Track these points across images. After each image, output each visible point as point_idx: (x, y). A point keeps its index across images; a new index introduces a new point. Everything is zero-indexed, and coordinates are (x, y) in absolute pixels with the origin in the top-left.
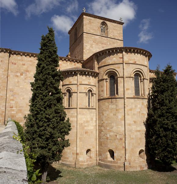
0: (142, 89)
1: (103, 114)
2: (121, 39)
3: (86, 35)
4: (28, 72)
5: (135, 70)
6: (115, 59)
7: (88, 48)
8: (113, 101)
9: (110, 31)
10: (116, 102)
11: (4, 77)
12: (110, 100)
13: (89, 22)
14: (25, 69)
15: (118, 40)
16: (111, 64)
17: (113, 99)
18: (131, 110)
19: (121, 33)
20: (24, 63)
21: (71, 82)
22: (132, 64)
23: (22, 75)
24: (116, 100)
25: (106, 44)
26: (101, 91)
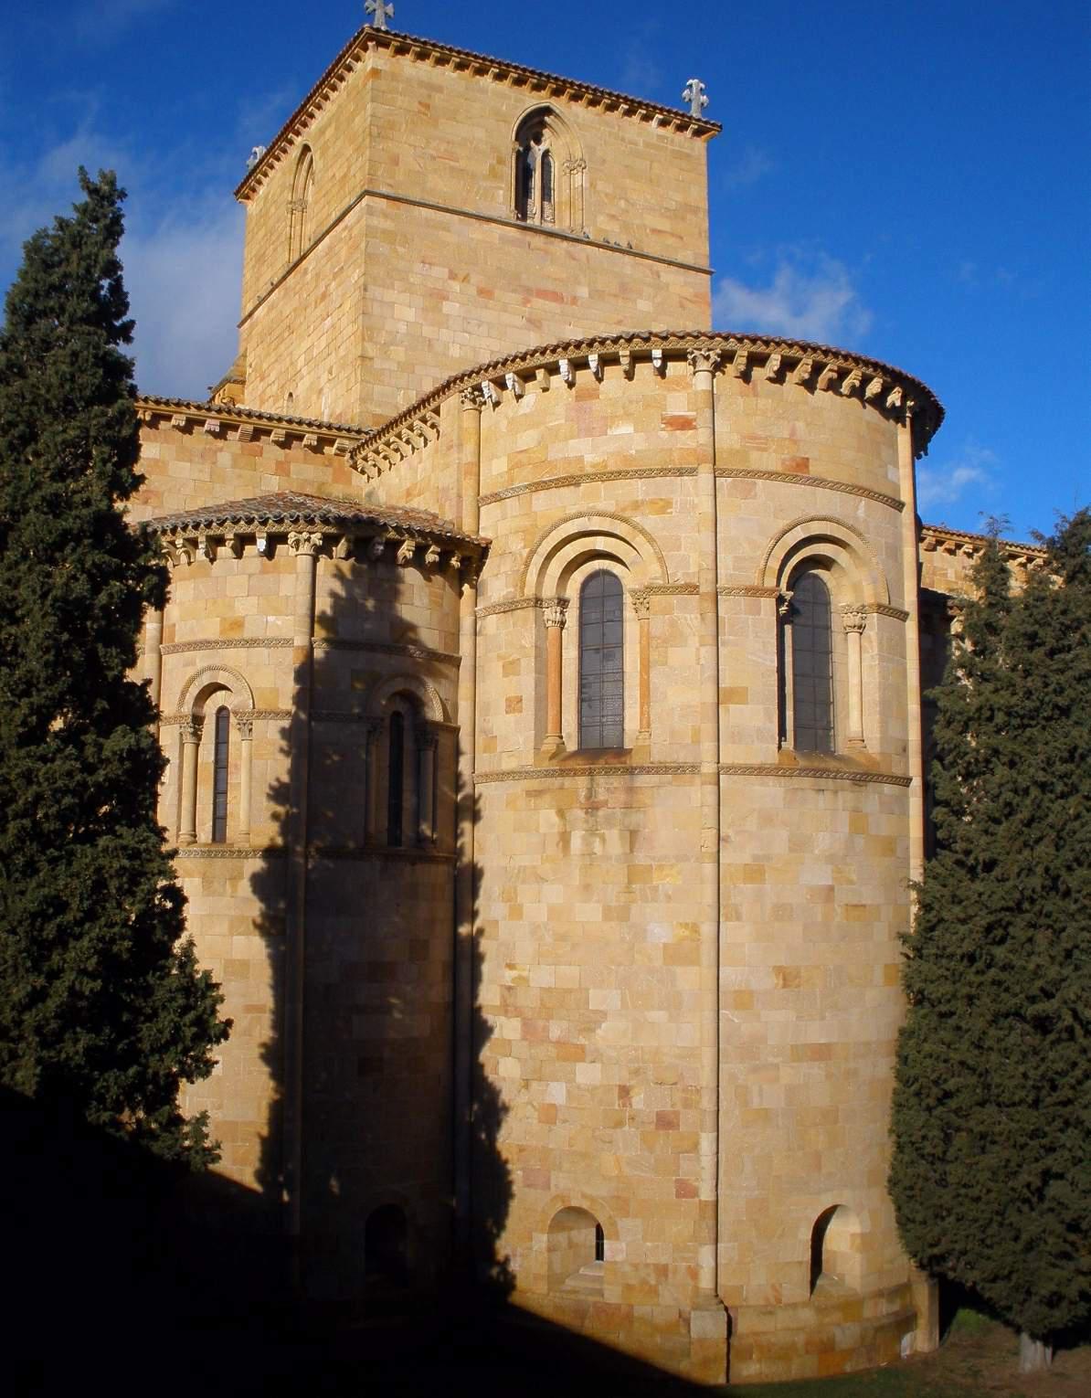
0: (854, 699)
1: (516, 912)
2: (690, 262)
3: (386, 216)
5: (799, 534)
6: (626, 429)
7: (403, 328)
8: (601, 795)
9: (600, 186)
10: (628, 807)
12: (582, 782)
13: (416, 107)
15: (670, 263)
16: (589, 470)
17: (601, 780)
18: (755, 872)
19: (695, 210)
21: (238, 624)
22: (770, 475)
24: (631, 790)
25: (556, 297)
26: (503, 705)
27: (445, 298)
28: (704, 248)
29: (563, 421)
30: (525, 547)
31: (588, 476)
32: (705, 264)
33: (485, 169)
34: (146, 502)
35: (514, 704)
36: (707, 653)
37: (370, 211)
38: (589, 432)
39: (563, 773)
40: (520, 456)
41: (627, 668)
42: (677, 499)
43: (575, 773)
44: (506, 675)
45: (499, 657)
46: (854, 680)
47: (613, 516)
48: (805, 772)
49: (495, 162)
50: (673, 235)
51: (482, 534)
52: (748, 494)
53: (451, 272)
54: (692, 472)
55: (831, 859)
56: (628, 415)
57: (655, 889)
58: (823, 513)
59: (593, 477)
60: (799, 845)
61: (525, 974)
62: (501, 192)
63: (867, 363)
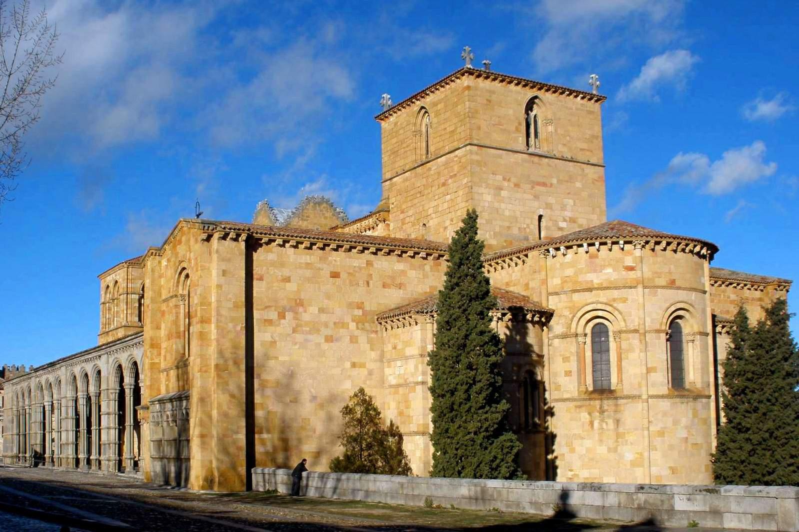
1: (572, 450)
3: (477, 154)
4: (302, 305)
5: (673, 308)
6: (609, 270)
7: (487, 205)
8: (606, 408)
9: (559, 131)
10: (616, 411)
11: (235, 327)
12: (597, 403)
14: (292, 297)
18: (661, 433)
19: (597, 137)
20: (288, 275)
22: (663, 287)
23: (284, 318)
24: (616, 405)
25: (544, 184)
26: (563, 374)
27: (502, 189)
28: (601, 155)
29: (584, 266)
30: (570, 314)
31: (596, 288)
32: (601, 162)
33: (514, 128)
34: (400, 288)
35: (568, 373)
36: (643, 355)
37: (471, 152)
38: (595, 271)
39: (590, 399)
40: (566, 278)
41: (611, 360)
42: (630, 297)
43: (595, 399)
44: (564, 362)
45: (561, 355)
46: (691, 360)
47: (606, 304)
48: (677, 396)
49: (517, 124)
50: (588, 150)
51: (550, 307)
52: (655, 294)
53: (503, 177)
54: (635, 287)
55: (686, 427)
56: (610, 265)
57: (627, 441)
58: (681, 299)
59: (598, 289)
60: (676, 422)
61: (577, 473)
62: (521, 138)
63: (696, 241)
